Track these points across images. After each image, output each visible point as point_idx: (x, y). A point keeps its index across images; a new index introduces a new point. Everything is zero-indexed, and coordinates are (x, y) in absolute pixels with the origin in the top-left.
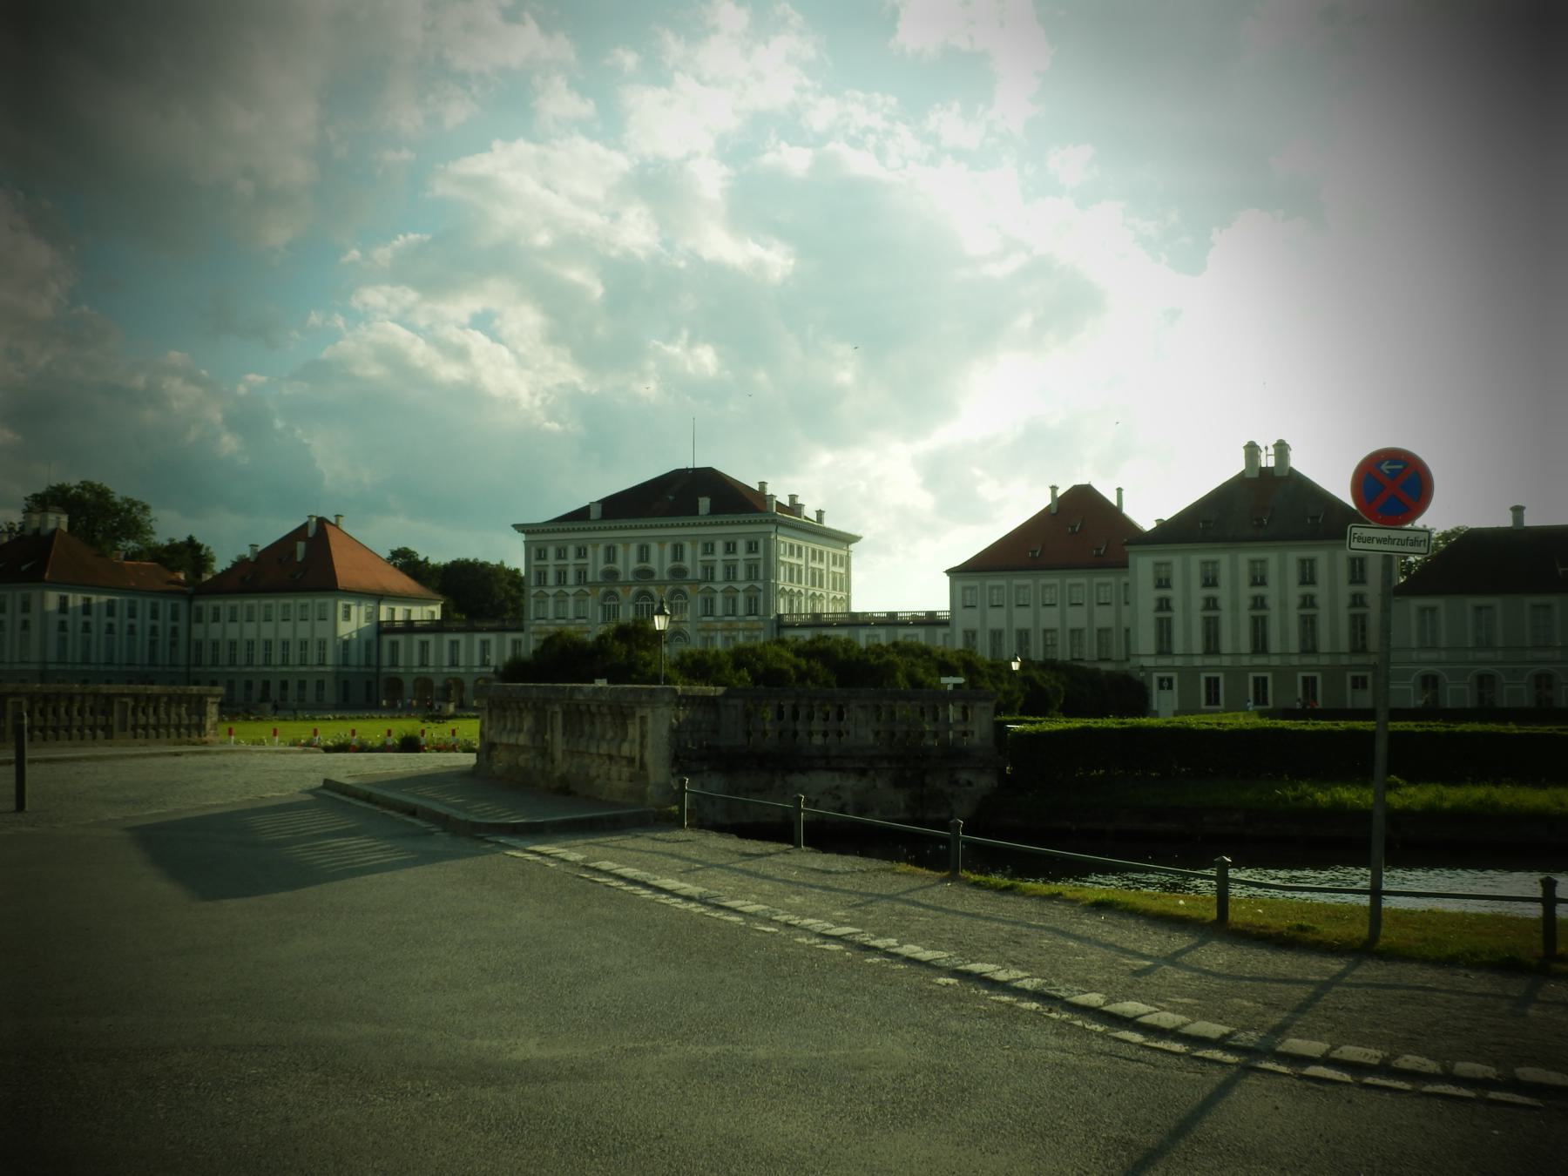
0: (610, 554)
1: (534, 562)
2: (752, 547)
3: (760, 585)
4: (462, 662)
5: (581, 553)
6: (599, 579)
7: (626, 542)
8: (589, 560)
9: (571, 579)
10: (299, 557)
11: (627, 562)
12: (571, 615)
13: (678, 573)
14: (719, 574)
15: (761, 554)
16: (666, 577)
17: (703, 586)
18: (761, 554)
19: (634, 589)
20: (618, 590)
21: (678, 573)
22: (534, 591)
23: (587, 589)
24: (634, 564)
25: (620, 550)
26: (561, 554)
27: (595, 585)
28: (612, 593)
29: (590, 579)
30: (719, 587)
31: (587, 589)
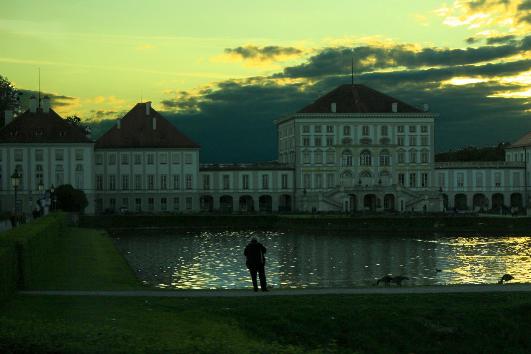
0: (347, 131)
1: (302, 133)
2: (424, 129)
3: (429, 148)
4: (251, 186)
5: (330, 129)
6: (341, 143)
7: (356, 124)
8: (335, 133)
9: (324, 142)
10: (155, 128)
11: (356, 135)
12: (324, 162)
13: (384, 141)
14: (407, 142)
15: (429, 133)
16: (378, 143)
17: (398, 148)
18: (429, 133)
19: (360, 149)
20: (351, 149)
21: (384, 141)
22: (302, 149)
23: (334, 149)
24: (360, 136)
25: (352, 128)
26: (318, 129)
27: (337, 146)
28: (347, 150)
29: (335, 143)
30: (407, 149)
31: (334, 149)
